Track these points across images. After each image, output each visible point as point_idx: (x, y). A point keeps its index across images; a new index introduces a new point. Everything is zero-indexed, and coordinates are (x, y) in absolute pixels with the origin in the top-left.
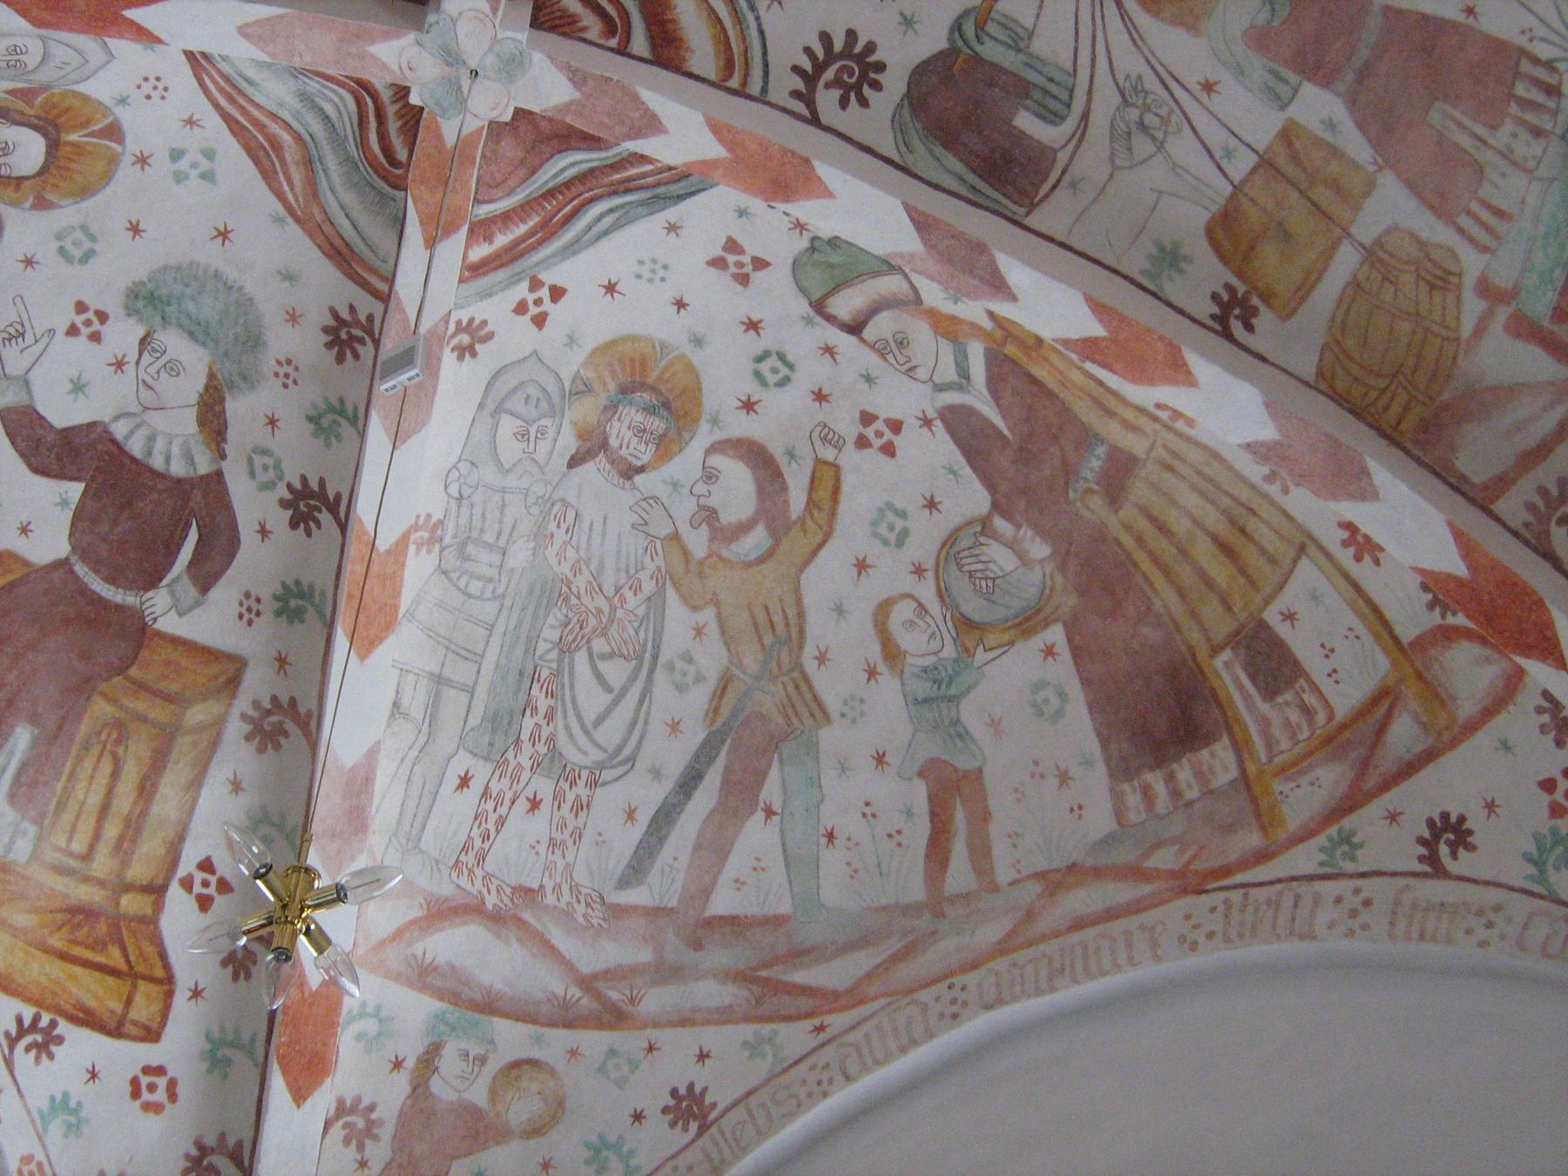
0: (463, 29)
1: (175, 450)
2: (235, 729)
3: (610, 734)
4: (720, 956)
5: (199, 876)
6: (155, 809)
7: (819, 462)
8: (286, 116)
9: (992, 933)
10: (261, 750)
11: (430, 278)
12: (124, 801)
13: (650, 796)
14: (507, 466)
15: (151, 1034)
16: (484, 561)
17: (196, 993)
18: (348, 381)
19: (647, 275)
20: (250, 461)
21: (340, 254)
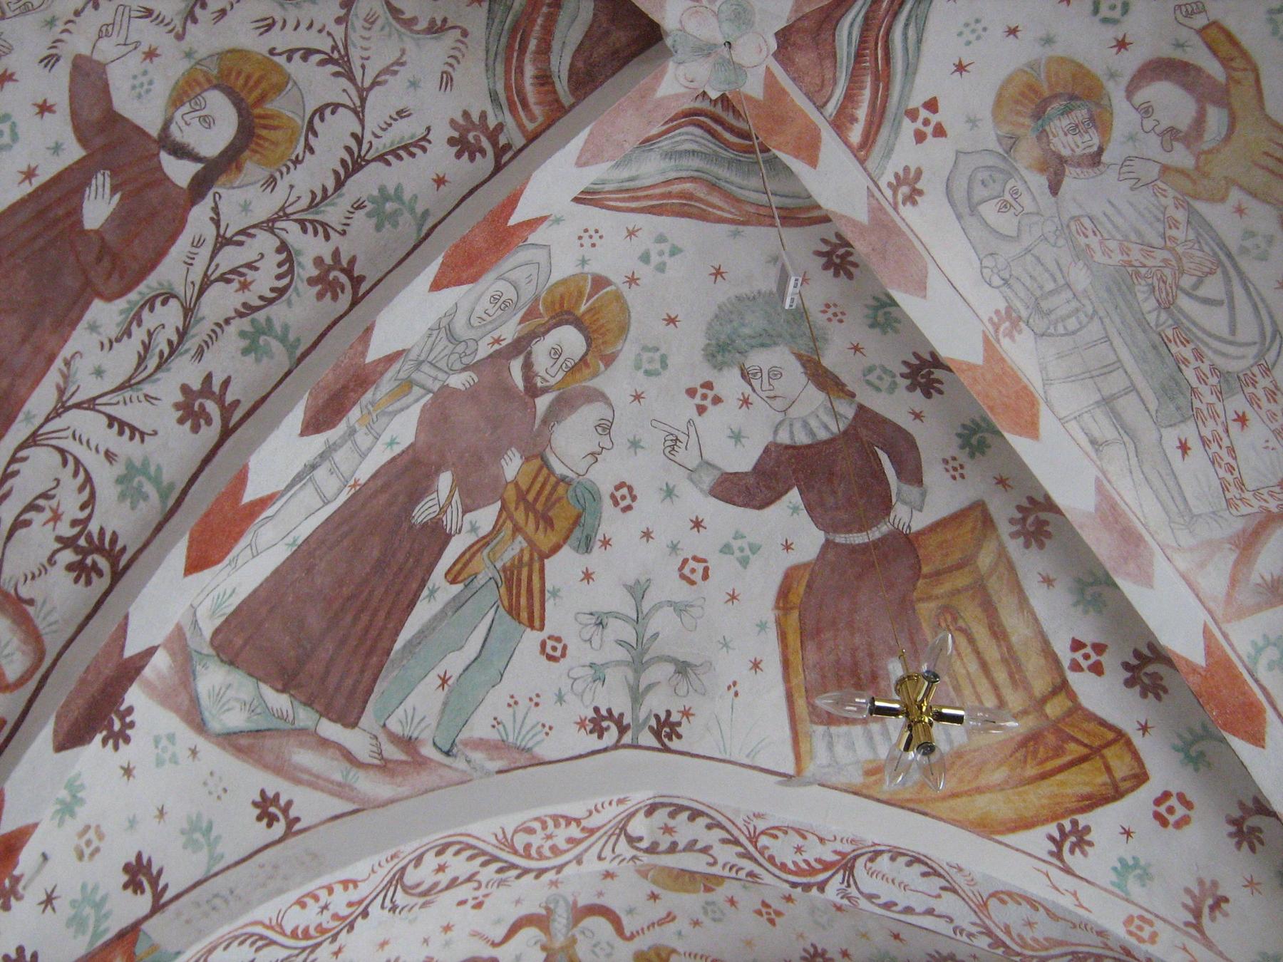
0: (692, 27)
2: (1014, 547)
3: (1247, 330)
5: (1078, 656)
6: (1014, 639)
7: (1201, 32)
8: (673, 175)
10: (1041, 546)
11: (835, 181)
12: (992, 653)
14: (1014, 234)
15: (1140, 778)
16: (1062, 305)
17: (1144, 728)
19: (972, 37)
20: (869, 383)
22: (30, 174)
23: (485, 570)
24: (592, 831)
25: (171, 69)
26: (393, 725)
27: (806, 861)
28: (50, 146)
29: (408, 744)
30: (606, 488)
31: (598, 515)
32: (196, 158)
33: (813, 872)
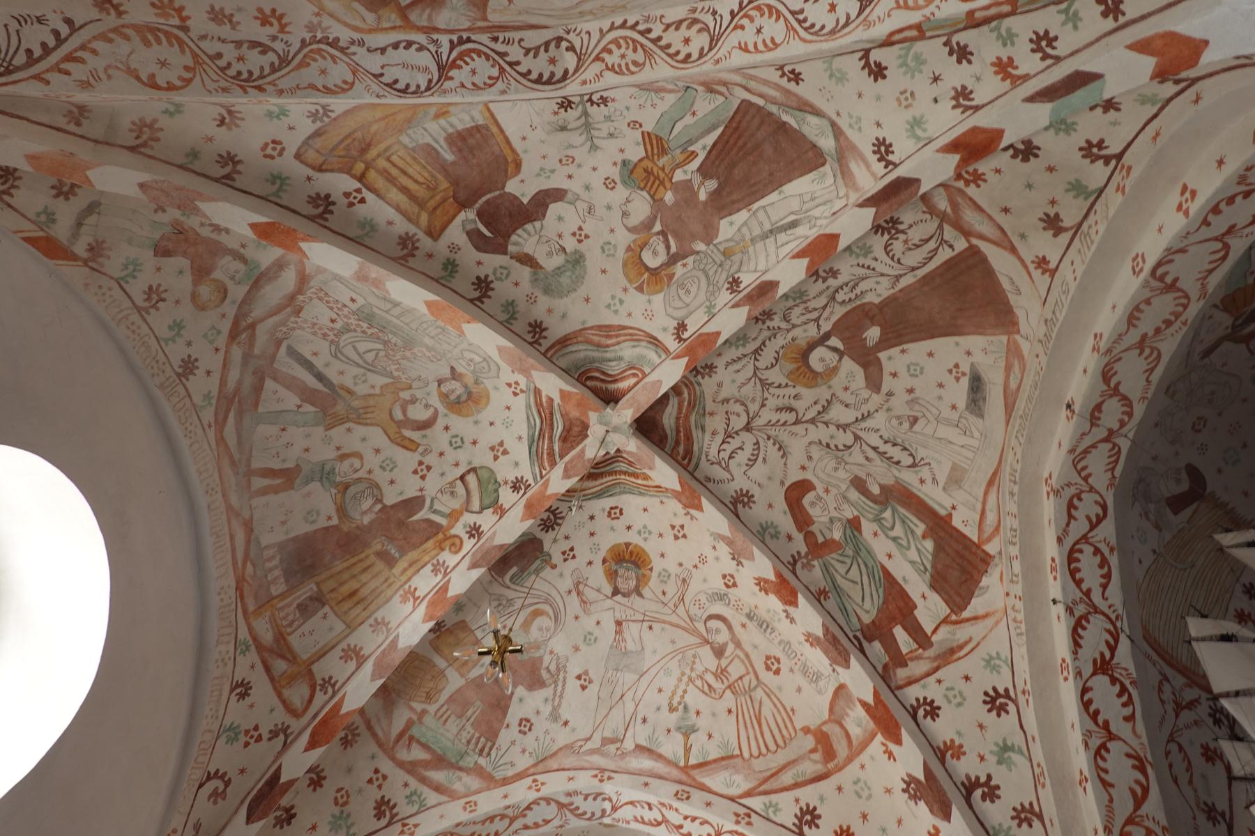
0: (623, 439)
1: (520, 240)
2: (412, 229)
3: (349, 351)
4: (249, 381)
5: (359, 196)
6: (395, 190)
7: (419, 445)
8: (617, 347)
9: (234, 500)
10: (400, 237)
12: (404, 181)
13: (319, 363)
15: (298, 156)
17: (309, 179)
18: (520, 326)
21: (564, 342)
22: (903, 351)
23: (678, 155)
24: (597, 58)
25: (837, 382)
26: (721, 99)
27: (467, 64)
28: (892, 359)
29: (712, 91)
30: (619, 186)
31: (621, 175)
32: (828, 347)
33: (461, 56)
